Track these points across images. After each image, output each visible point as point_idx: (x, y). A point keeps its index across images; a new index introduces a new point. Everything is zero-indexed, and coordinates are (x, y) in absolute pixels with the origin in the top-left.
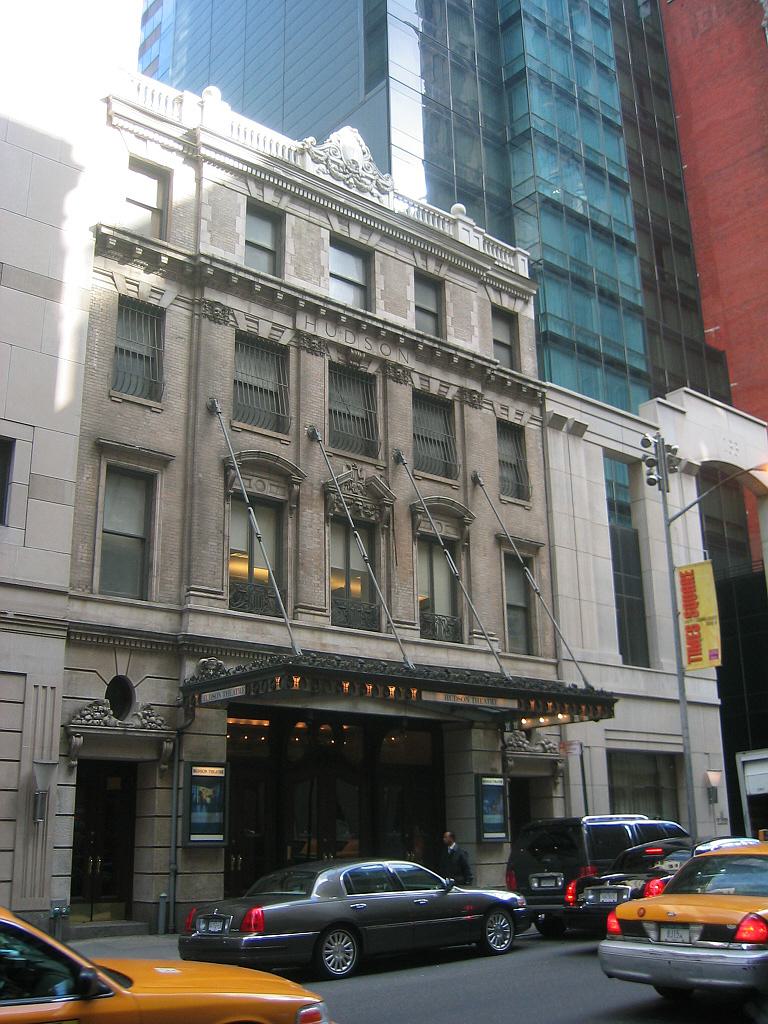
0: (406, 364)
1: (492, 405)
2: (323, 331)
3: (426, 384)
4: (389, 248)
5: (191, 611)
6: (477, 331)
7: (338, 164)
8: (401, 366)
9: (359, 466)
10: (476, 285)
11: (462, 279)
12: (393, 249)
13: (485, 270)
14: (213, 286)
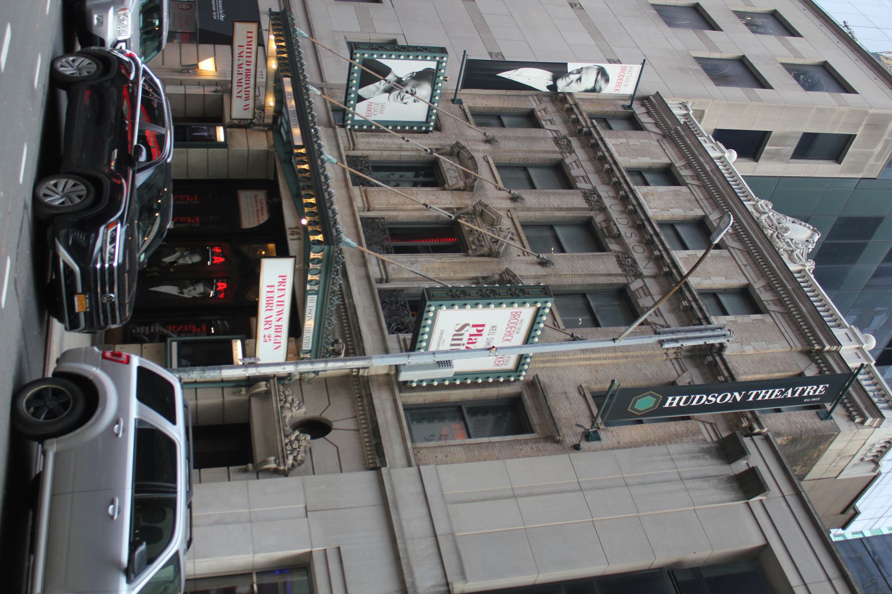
0: (641, 267)
1: (684, 372)
2: (609, 202)
3: (643, 295)
4: (741, 259)
5: (334, 129)
6: (749, 350)
7: (771, 221)
8: (636, 263)
9: (515, 237)
10: (799, 347)
11: (788, 329)
12: (745, 263)
13: (820, 343)
14: (579, 140)
